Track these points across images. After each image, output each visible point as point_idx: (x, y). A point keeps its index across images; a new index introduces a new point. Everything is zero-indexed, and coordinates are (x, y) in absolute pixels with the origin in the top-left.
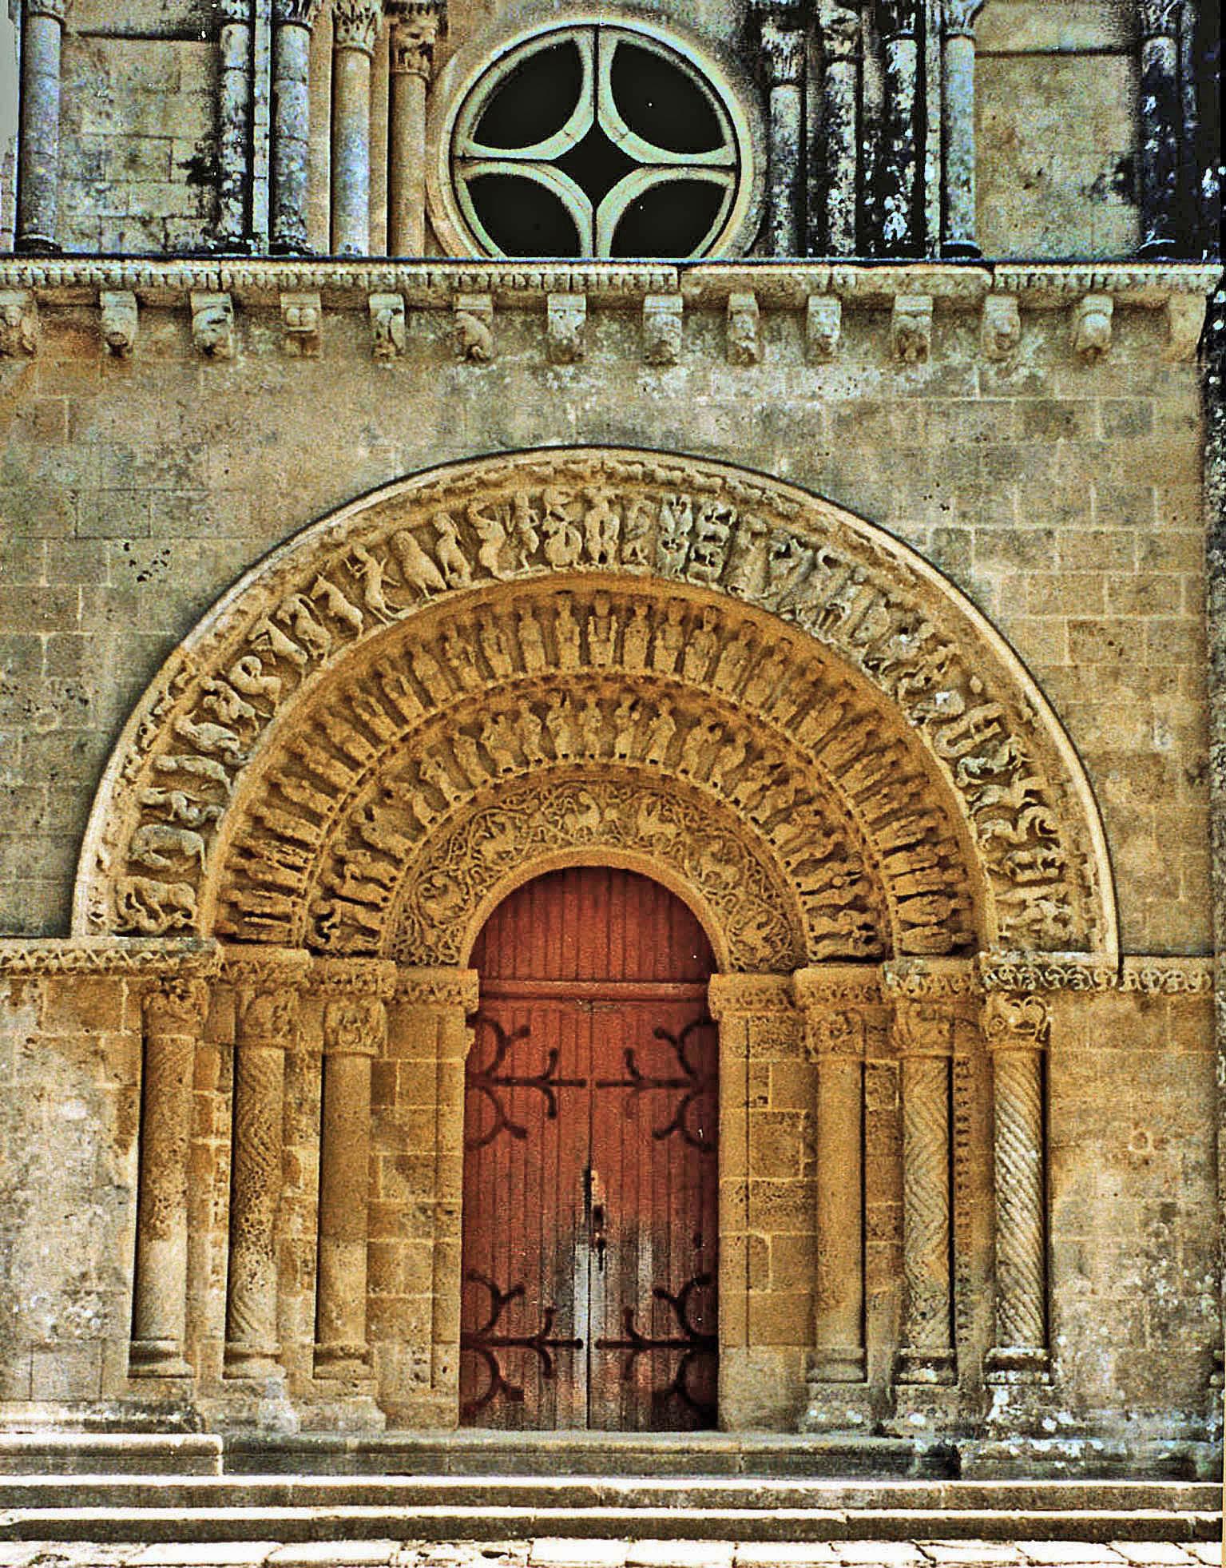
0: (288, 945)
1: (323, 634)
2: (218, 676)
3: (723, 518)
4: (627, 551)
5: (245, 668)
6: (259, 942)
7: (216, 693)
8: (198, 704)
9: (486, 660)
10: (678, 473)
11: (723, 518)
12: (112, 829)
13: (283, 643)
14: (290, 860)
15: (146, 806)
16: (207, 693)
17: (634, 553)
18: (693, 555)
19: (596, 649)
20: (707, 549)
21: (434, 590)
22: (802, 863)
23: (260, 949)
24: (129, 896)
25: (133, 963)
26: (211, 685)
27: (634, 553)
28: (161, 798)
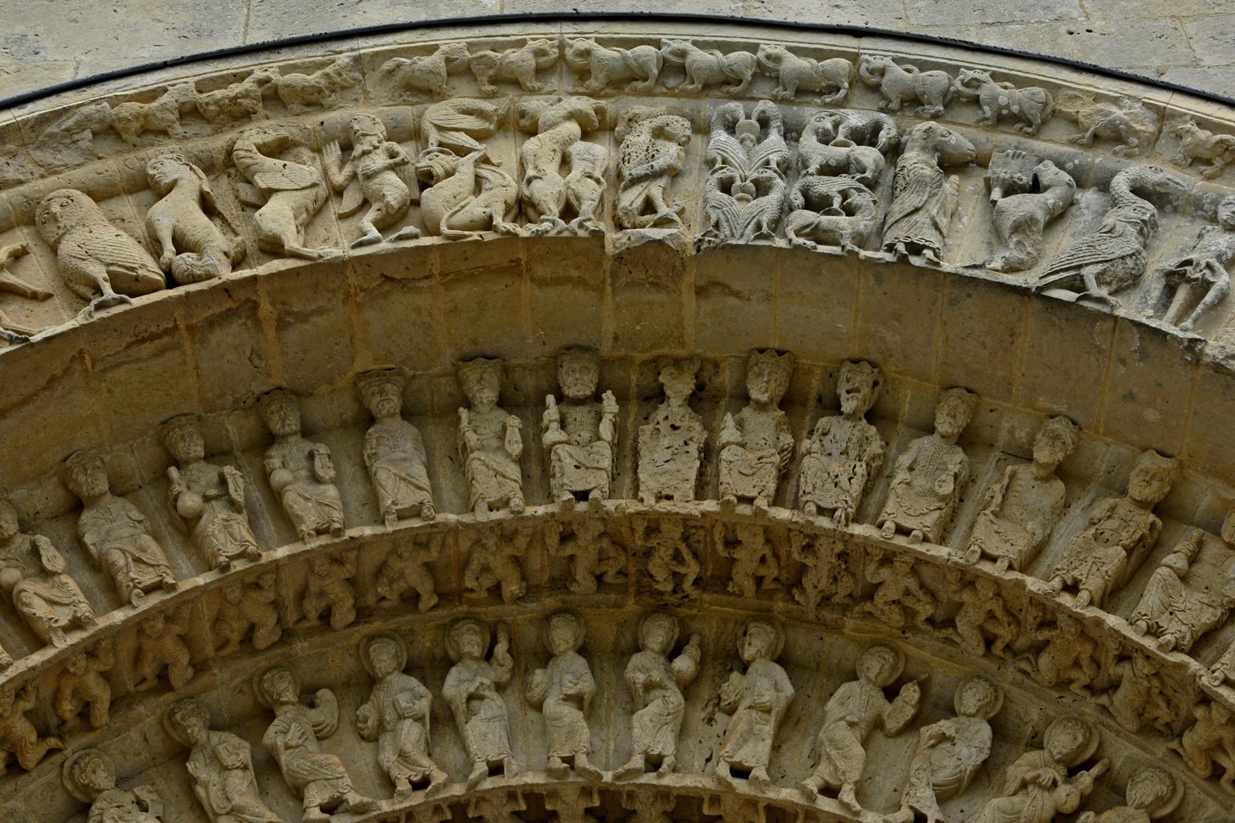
9: (275, 497)
11: (866, 136)
19: (566, 457)
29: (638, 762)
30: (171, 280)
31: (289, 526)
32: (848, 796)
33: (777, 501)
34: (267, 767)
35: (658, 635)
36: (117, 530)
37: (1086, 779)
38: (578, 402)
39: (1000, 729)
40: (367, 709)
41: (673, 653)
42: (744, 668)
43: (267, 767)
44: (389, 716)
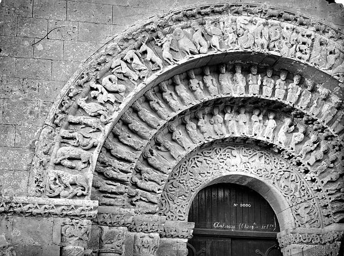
0: (123, 207)
1: (143, 66)
2: (98, 82)
3: (309, 36)
4: (272, 45)
5: (110, 80)
6: (110, 205)
7: (97, 89)
8: (88, 94)
10: (291, 16)
12: (48, 146)
13: (125, 69)
14: (124, 168)
15: (63, 138)
16: (92, 89)
17: (274, 46)
18: (298, 49)
20: (303, 47)
21: (192, 53)
22: (329, 182)
23: (110, 207)
24: (55, 179)
25: (57, 210)
26: (95, 86)
27: (274, 46)
28: (71, 135)
29: (253, 135)
30: (199, 53)
31: (209, 93)
32: (283, 145)
33: (283, 99)
34: (198, 127)
35: (257, 113)
36: (182, 89)
37: (316, 145)
38: (254, 75)
39: (305, 133)
40: (212, 120)
41: (258, 116)
42: (269, 119)
43: (198, 127)
44: (216, 121)
